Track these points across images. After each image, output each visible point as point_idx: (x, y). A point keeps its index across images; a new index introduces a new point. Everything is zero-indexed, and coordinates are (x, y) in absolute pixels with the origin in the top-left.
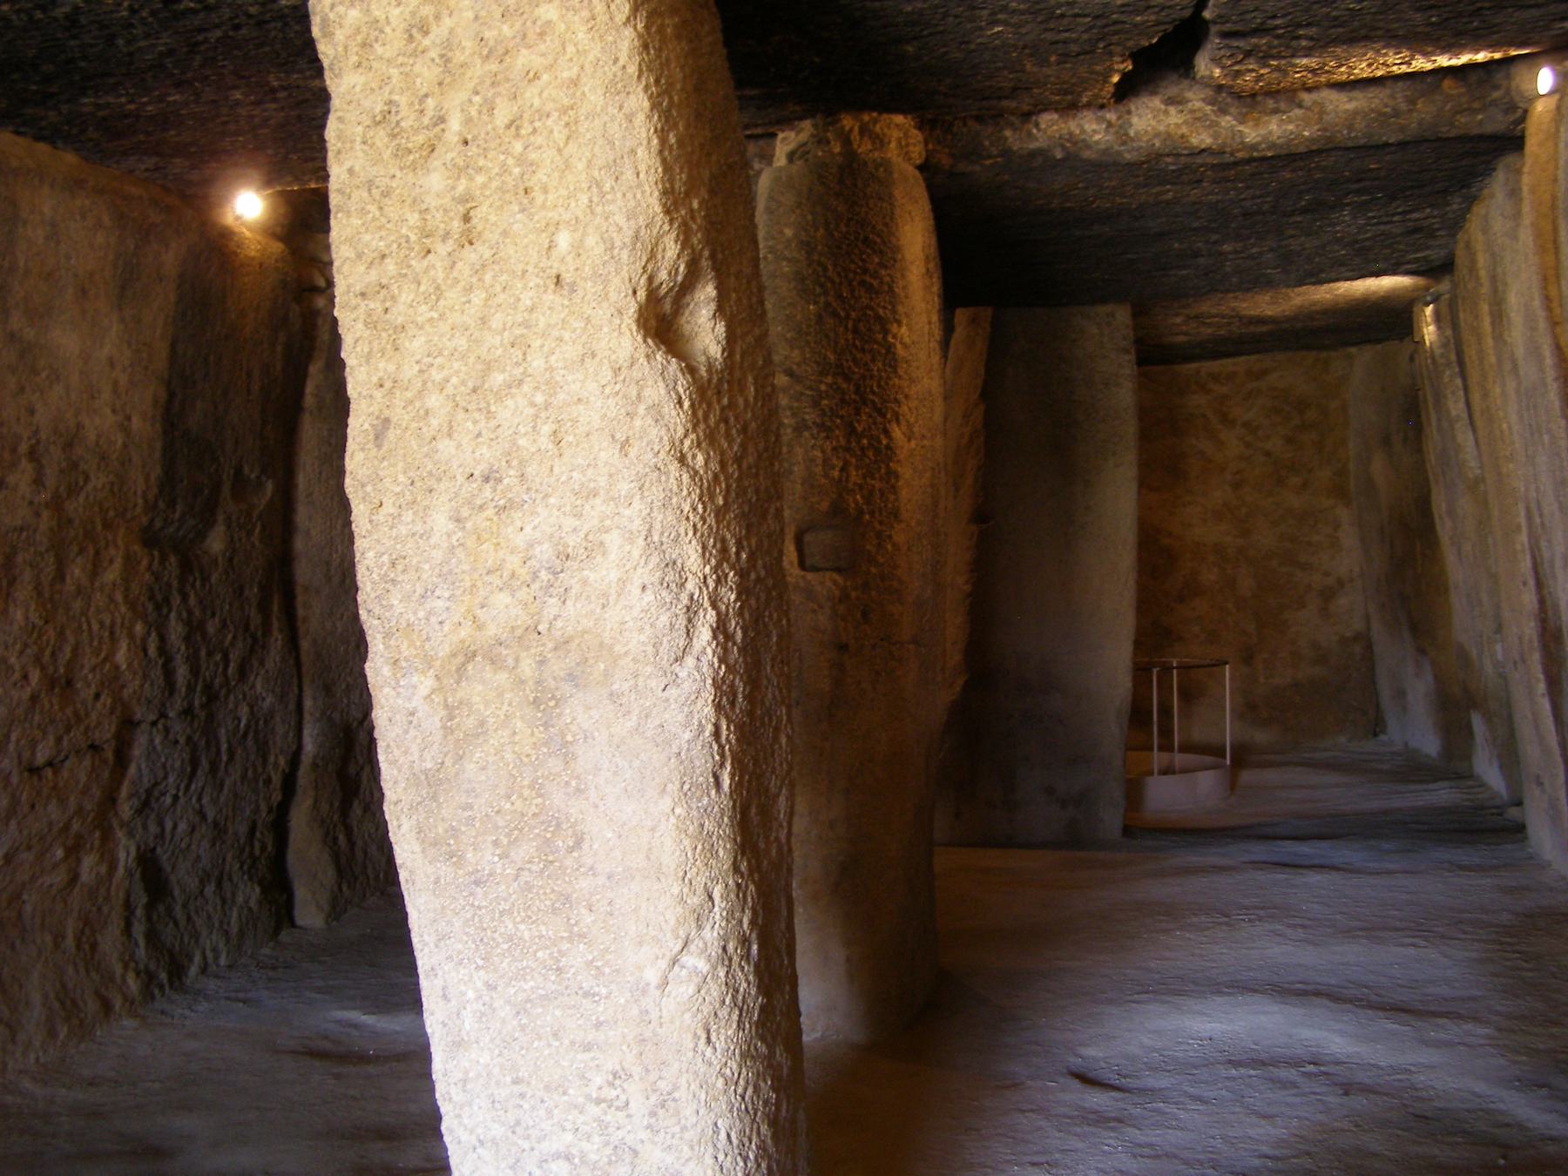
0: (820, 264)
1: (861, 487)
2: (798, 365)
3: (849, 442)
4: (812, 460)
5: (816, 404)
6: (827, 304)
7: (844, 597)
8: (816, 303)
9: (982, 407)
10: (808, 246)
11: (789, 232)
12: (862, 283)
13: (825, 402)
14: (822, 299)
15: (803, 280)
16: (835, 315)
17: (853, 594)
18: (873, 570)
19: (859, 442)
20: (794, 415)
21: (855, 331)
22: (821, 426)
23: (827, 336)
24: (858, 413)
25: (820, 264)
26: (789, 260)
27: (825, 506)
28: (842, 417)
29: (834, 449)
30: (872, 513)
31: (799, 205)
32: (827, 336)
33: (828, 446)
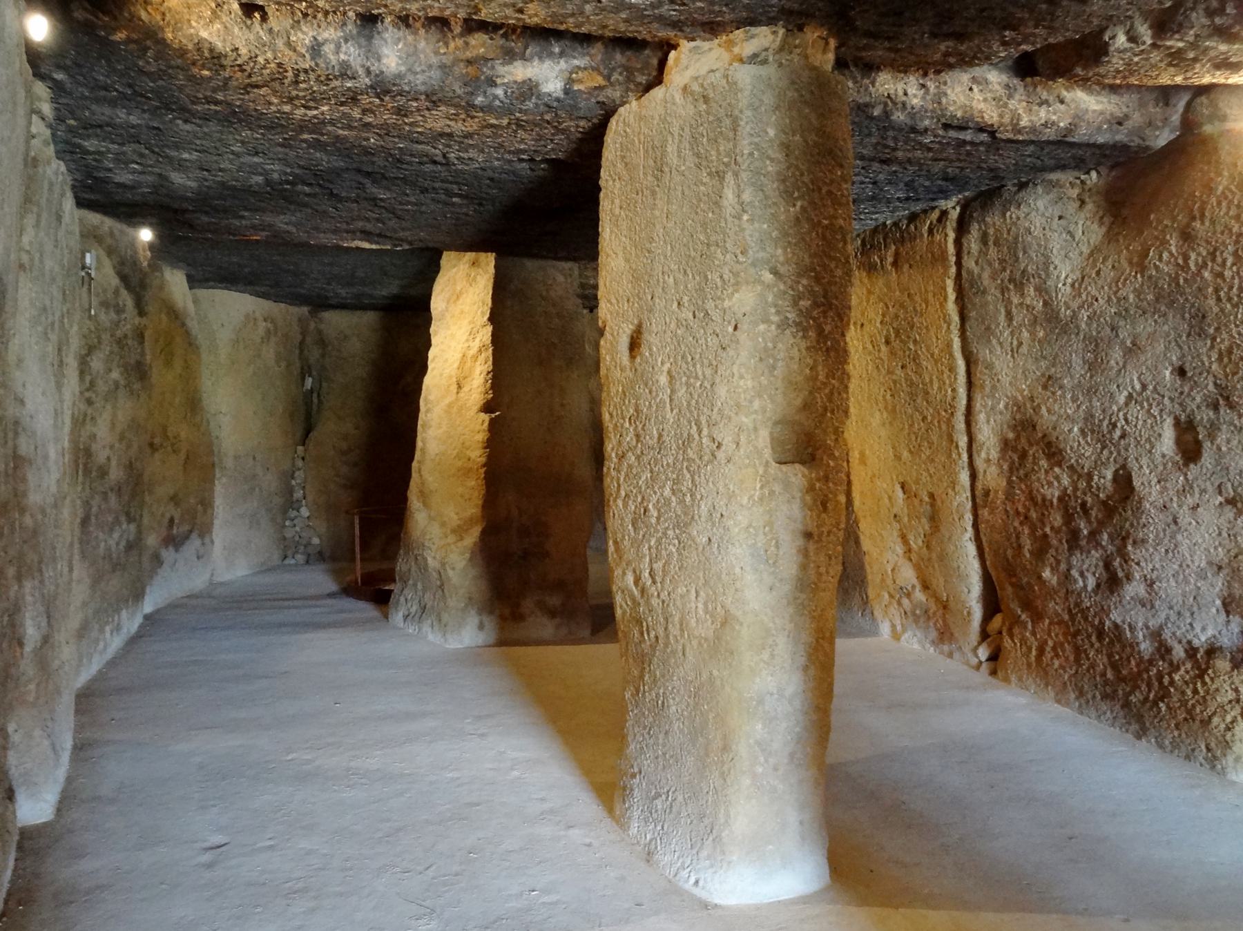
0: (797, 167)
1: (824, 384)
2: (782, 264)
3: (818, 342)
4: (792, 358)
5: (795, 303)
6: (803, 209)
7: (811, 489)
8: (794, 205)
9: (490, 328)
10: (786, 147)
11: (772, 132)
12: (830, 193)
13: (802, 303)
14: (799, 204)
15: (784, 181)
16: (809, 219)
17: (818, 485)
18: (832, 463)
19: (825, 343)
20: (778, 313)
21: (824, 238)
22: (797, 324)
23: (803, 239)
24: (825, 317)
25: (797, 167)
26: (772, 160)
27: (798, 402)
28: (814, 319)
29: (808, 349)
30: (832, 412)
31: (777, 108)
32: (803, 239)
33: (803, 345)
